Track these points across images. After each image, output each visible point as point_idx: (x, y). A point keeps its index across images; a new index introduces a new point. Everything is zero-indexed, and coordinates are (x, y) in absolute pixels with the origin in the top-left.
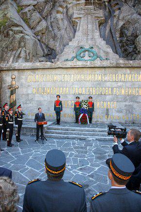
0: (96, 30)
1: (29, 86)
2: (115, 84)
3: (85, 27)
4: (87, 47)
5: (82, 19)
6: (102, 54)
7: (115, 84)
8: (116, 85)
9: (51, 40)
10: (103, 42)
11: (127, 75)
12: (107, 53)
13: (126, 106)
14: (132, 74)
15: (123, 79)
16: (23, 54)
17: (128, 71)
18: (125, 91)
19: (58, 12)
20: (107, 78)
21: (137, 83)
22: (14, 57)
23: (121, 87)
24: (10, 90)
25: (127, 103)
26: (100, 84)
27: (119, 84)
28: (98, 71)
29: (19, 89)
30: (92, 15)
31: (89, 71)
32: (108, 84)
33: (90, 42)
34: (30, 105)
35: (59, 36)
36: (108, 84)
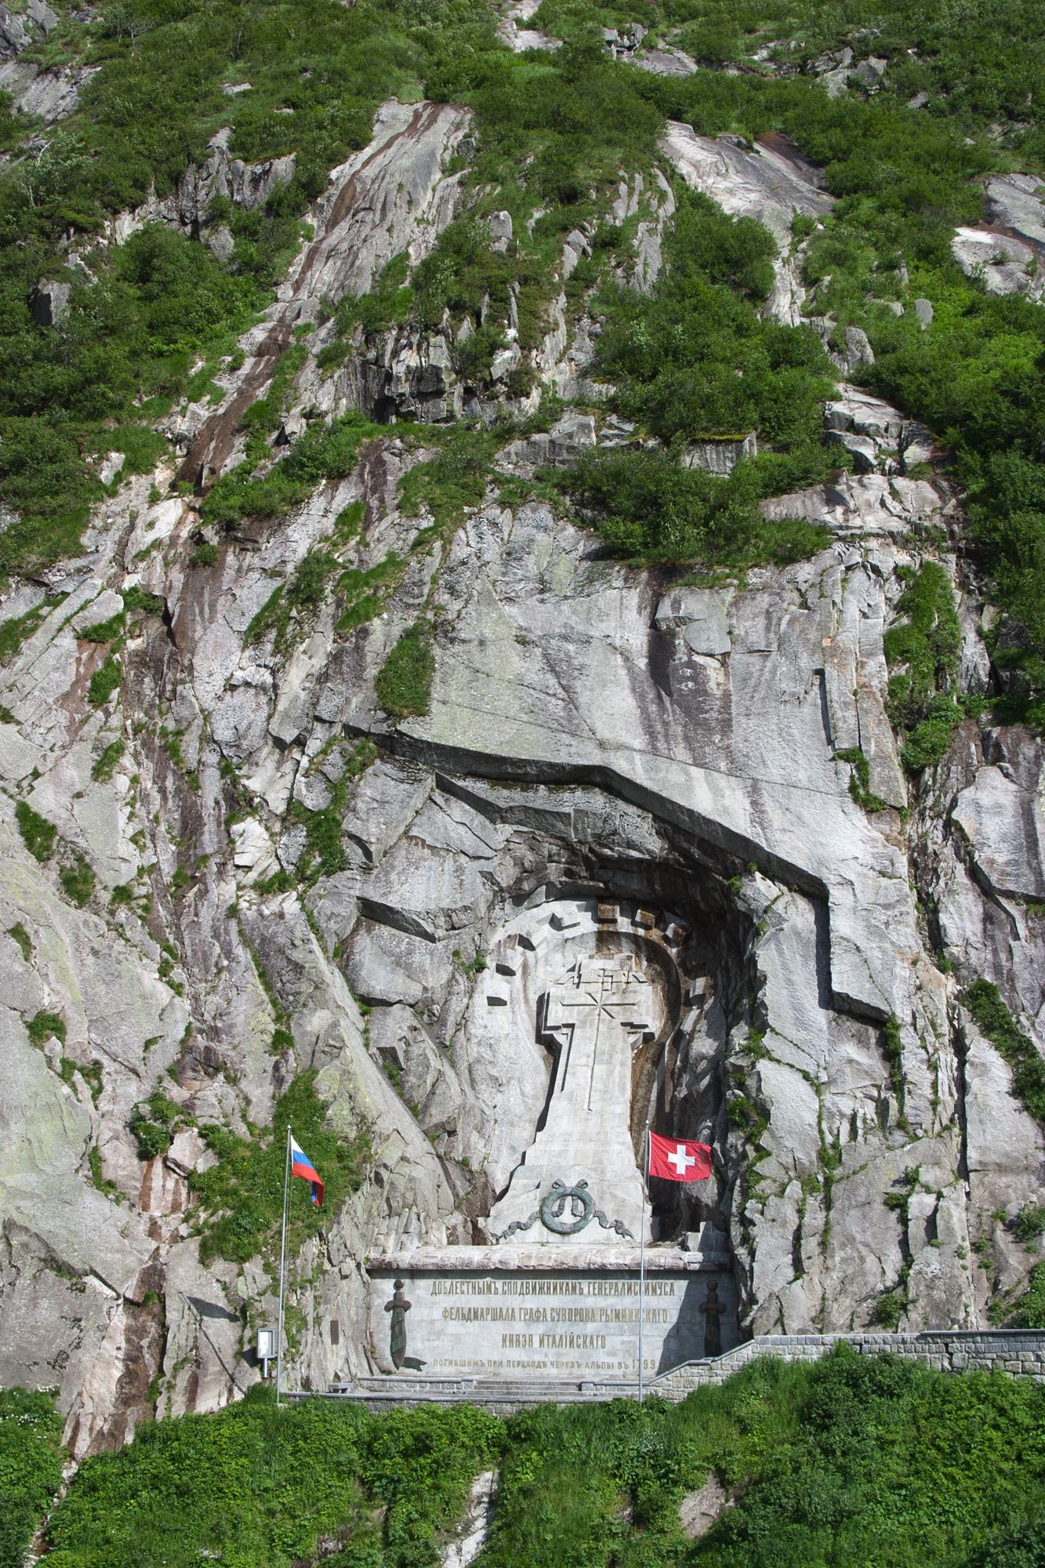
13: (623, 1342)
25: (625, 1338)
30: (614, 1010)
34: (437, 1343)
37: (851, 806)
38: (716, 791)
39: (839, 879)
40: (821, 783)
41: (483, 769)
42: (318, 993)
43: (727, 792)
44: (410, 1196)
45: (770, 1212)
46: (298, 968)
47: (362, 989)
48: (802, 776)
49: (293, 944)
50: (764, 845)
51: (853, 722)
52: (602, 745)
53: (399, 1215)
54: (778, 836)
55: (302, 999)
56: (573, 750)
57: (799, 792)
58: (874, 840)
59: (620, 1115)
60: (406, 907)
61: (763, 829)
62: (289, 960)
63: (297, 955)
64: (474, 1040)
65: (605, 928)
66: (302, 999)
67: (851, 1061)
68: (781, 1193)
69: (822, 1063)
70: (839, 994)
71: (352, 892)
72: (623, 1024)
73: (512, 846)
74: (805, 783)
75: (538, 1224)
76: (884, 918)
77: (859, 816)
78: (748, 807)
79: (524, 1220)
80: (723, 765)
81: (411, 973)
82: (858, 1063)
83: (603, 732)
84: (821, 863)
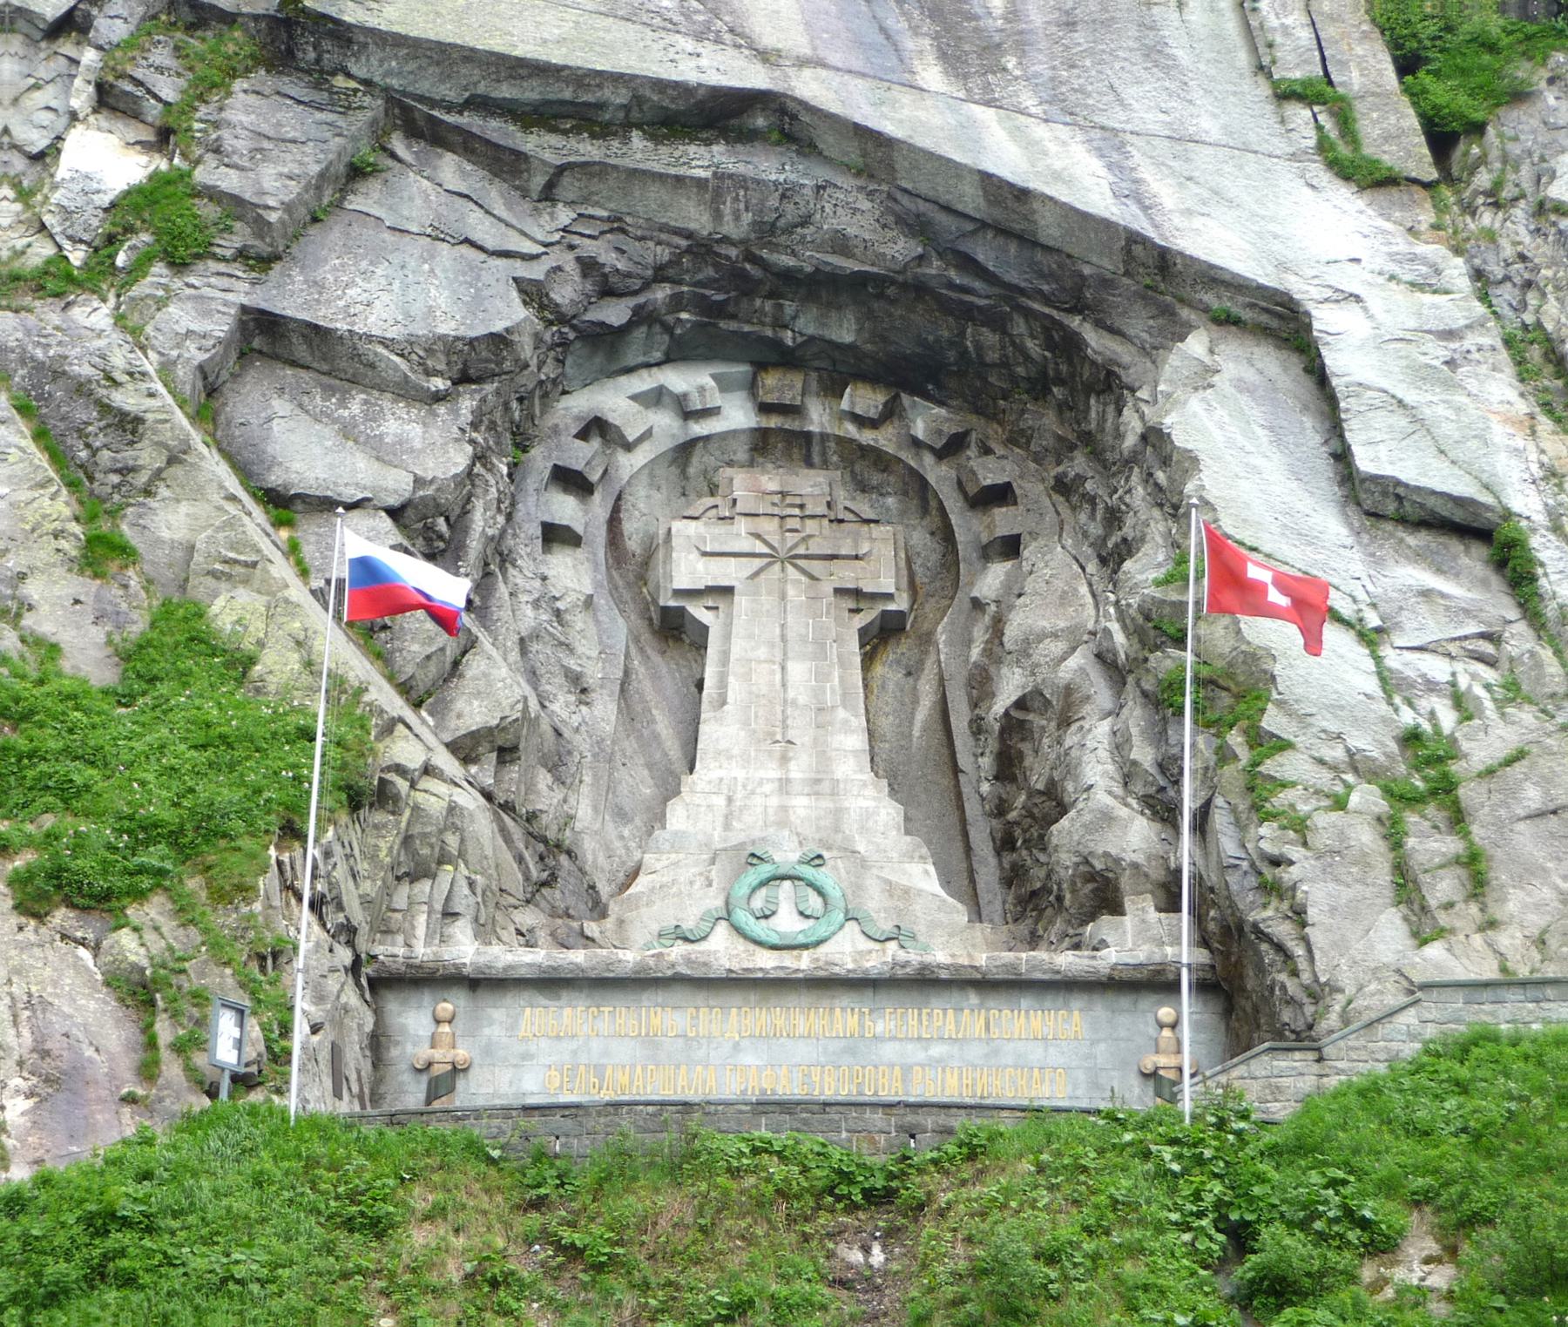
0: (841, 713)
1: (527, 1056)
2: (916, 1053)
3: (766, 677)
4: (787, 855)
5: (741, 601)
6: (874, 902)
7: (916, 1053)
8: (921, 1056)
9: (544, 779)
10: (888, 812)
11: (967, 1012)
12: (901, 894)
14: (988, 1010)
15: (950, 1028)
16: (464, 900)
17: (974, 998)
18: (960, 1078)
19: (555, 535)
20: (881, 1027)
21: (1011, 1045)
22: (429, 913)
23: (940, 1063)
24: (424, 1078)
26: (851, 1051)
27: (937, 1050)
28: (845, 1000)
29: (472, 1073)
30: (816, 567)
31: (806, 998)
32: (889, 1051)
33: (801, 805)
35: (582, 743)
36: (889, 1051)
37: (1324, 177)
38: (1031, 146)
39: (1329, 293)
40: (1252, 137)
41: (505, 91)
42: (177, 471)
43: (1052, 148)
44: (452, 841)
45: (1321, 840)
46: (128, 425)
47: (274, 479)
48: (1208, 126)
49: (109, 378)
50: (1150, 233)
51: (1305, 35)
52: (766, 56)
53: (433, 876)
54: (1177, 220)
55: (142, 479)
56: (704, 62)
57: (1210, 150)
58: (1384, 232)
59: (855, 752)
60: (359, 328)
61: (1146, 209)
62: (105, 408)
63: (126, 399)
64: (524, 598)
65: (774, 422)
66: (142, 479)
67: (1426, 594)
68: (1340, 804)
69: (1362, 596)
70: (1375, 479)
71: (230, 297)
72: (839, 592)
73: (576, 240)
74: (1215, 134)
75: (722, 929)
76: (1445, 354)
77: (1343, 196)
78: (1103, 172)
79: (688, 924)
80: (1028, 100)
81: (382, 453)
82: (1443, 595)
83: (768, 38)
84: (1282, 266)
